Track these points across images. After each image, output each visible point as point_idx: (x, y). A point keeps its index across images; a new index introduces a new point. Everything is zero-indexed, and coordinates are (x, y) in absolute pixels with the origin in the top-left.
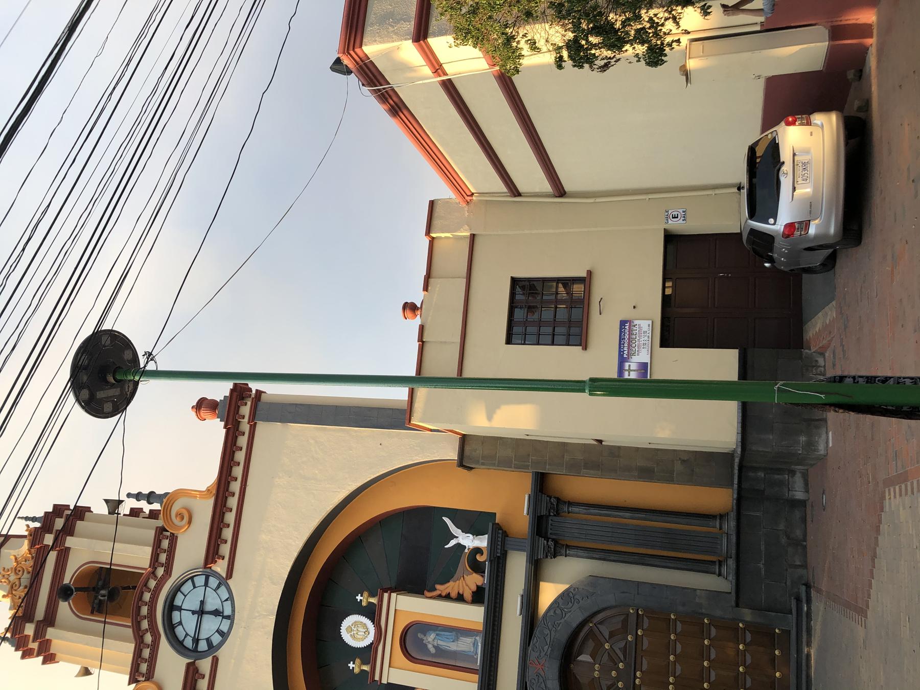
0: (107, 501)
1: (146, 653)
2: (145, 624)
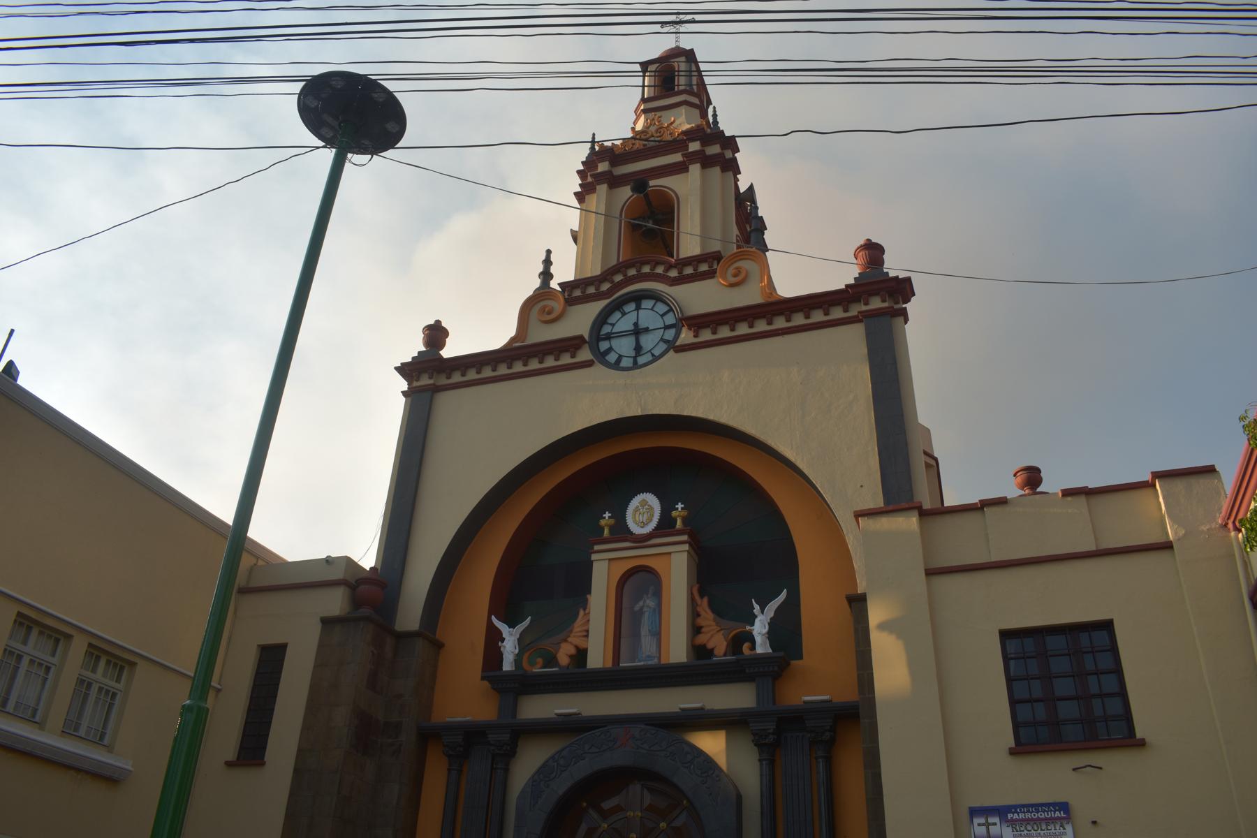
0: (751, 189)
1: (591, 290)
2: (618, 278)
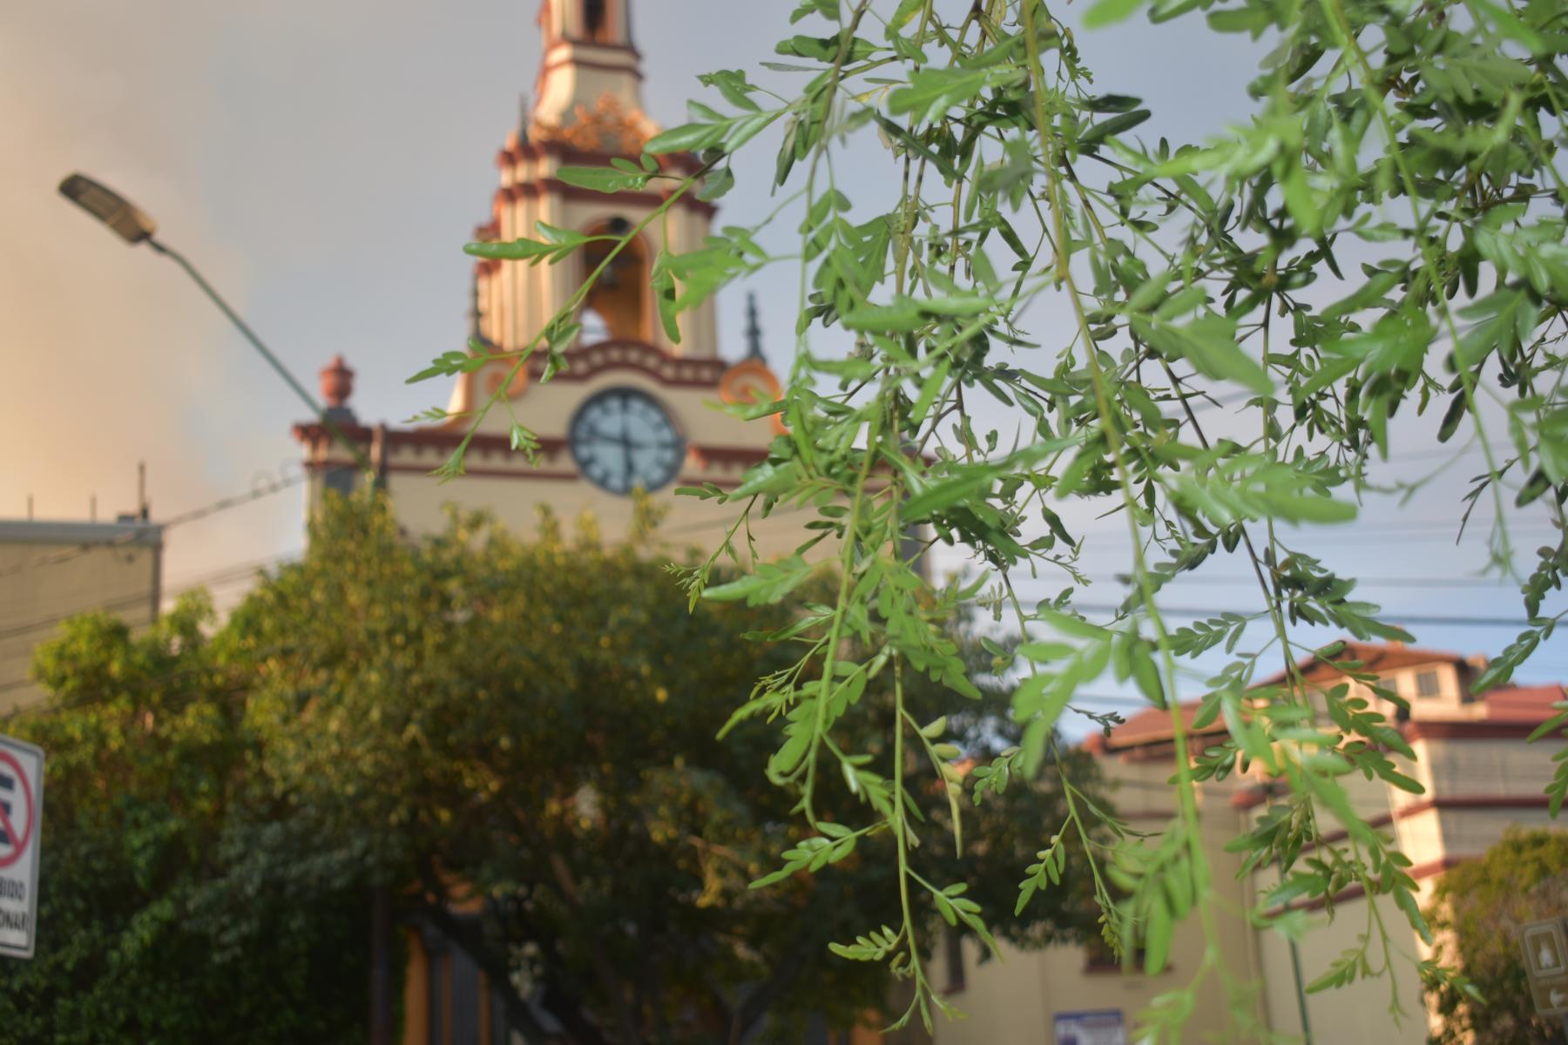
2: (597, 358)
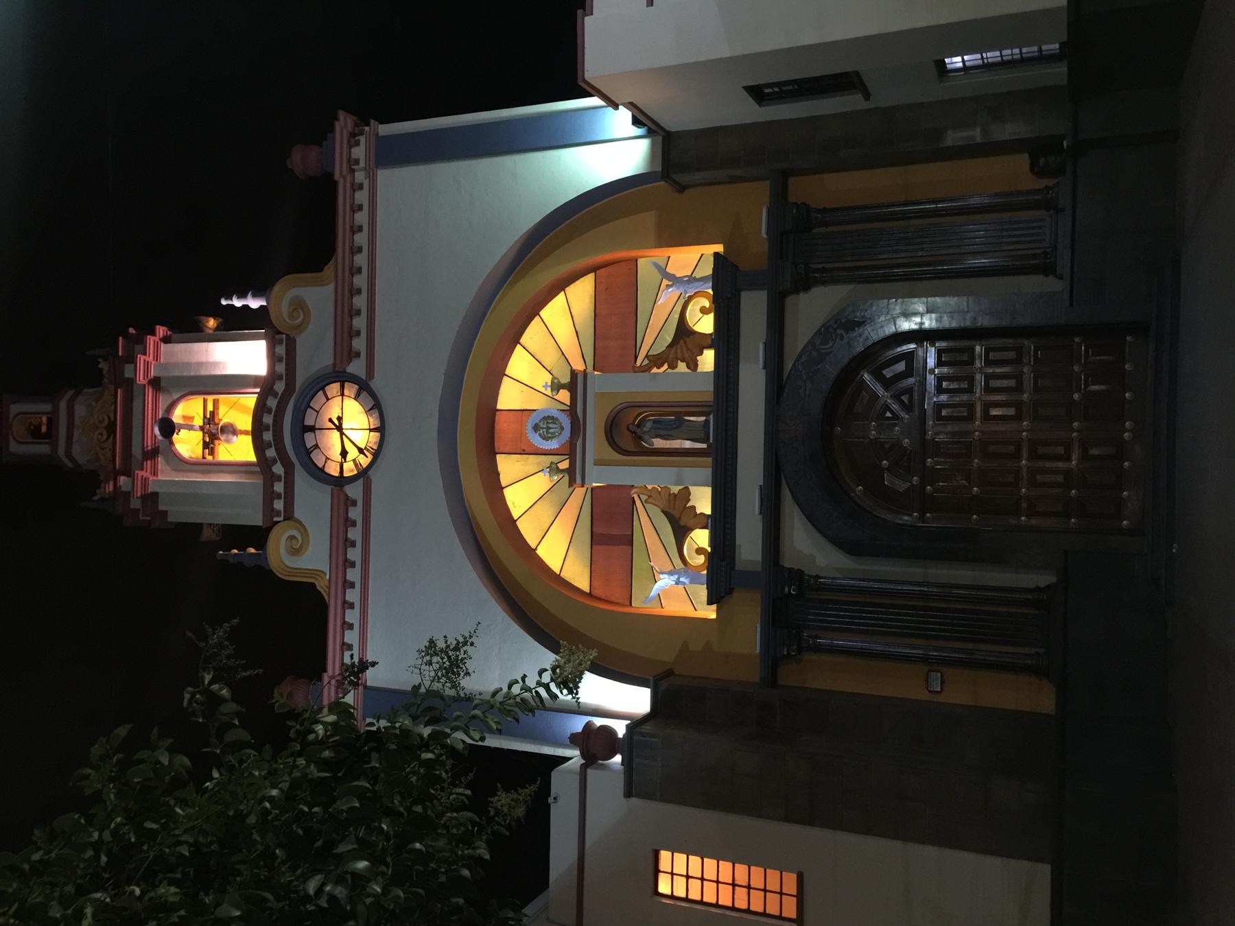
1: (279, 487)
